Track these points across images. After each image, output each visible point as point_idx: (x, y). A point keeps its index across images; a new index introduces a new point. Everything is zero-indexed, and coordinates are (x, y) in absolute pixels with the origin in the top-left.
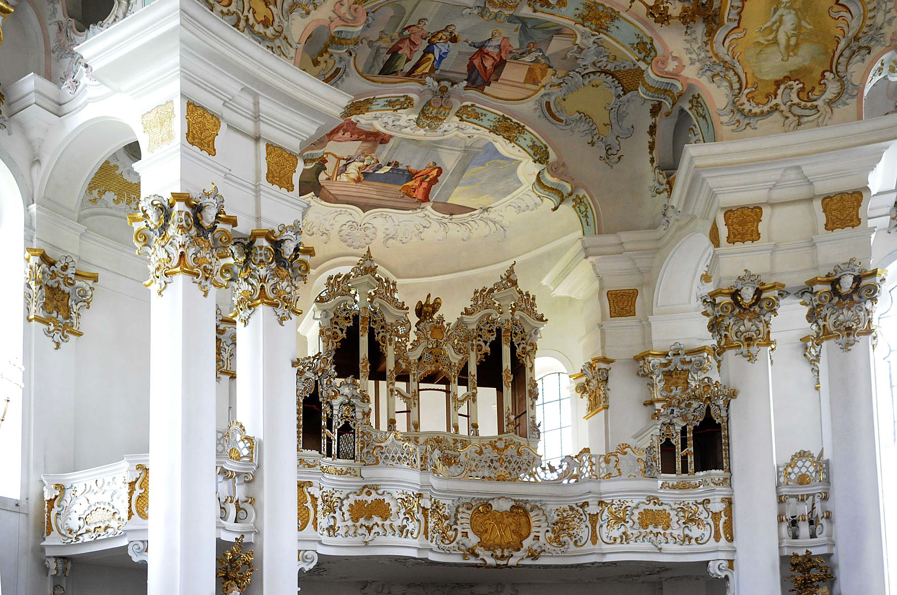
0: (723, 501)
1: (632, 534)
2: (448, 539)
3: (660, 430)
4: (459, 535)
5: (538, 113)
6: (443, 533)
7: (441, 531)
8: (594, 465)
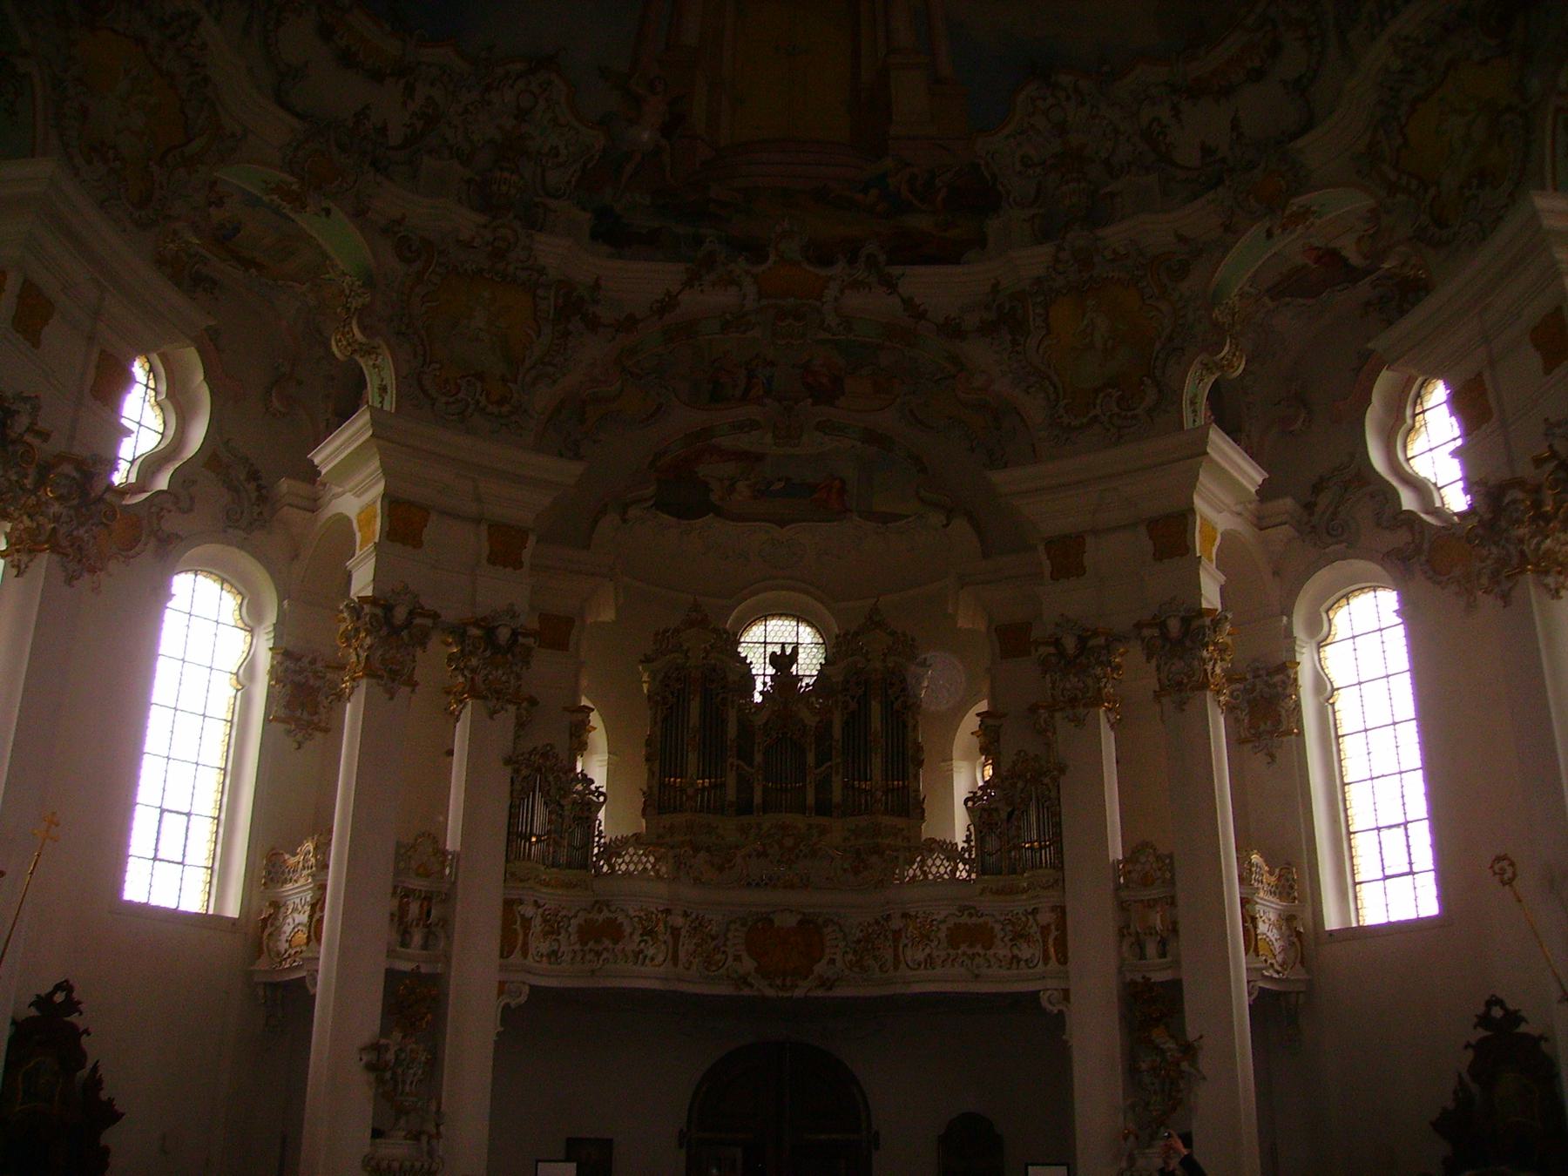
0: (1053, 909)
4: (730, 959)
6: (707, 957)
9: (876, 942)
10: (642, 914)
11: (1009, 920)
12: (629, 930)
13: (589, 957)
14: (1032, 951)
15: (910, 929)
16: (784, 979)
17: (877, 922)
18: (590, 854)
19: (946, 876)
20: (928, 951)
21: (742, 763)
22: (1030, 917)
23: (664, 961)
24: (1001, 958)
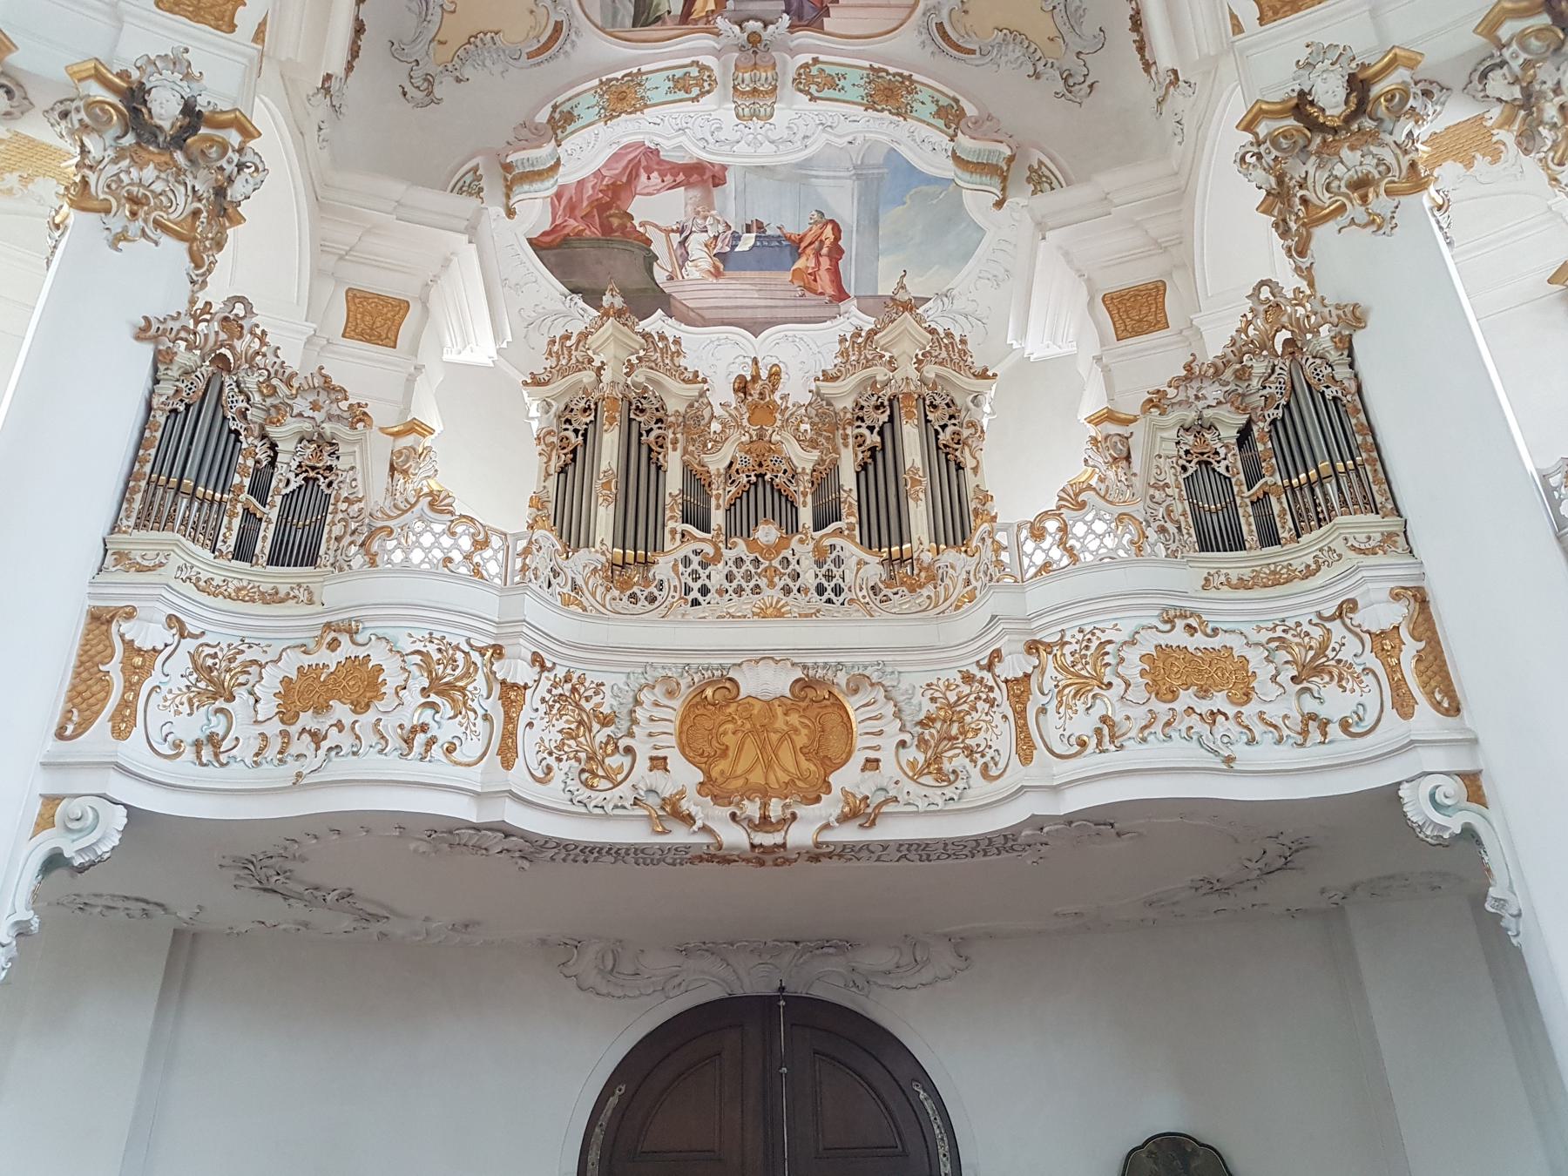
1: (1128, 718)
2: (607, 777)
3: (1178, 443)
4: (642, 763)
5: (931, 48)
6: (589, 759)
7: (583, 755)
8: (1005, 548)
9: (968, 719)
10: (432, 649)
11: (1280, 638)
12: (392, 678)
13: (294, 749)
14: (1356, 697)
15: (1051, 671)
16: (765, 806)
17: (968, 678)
18: (325, 536)
19: (1121, 553)
20: (1098, 710)
21: (689, 527)
22: (1336, 626)
23: (484, 754)
24: (1280, 723)
